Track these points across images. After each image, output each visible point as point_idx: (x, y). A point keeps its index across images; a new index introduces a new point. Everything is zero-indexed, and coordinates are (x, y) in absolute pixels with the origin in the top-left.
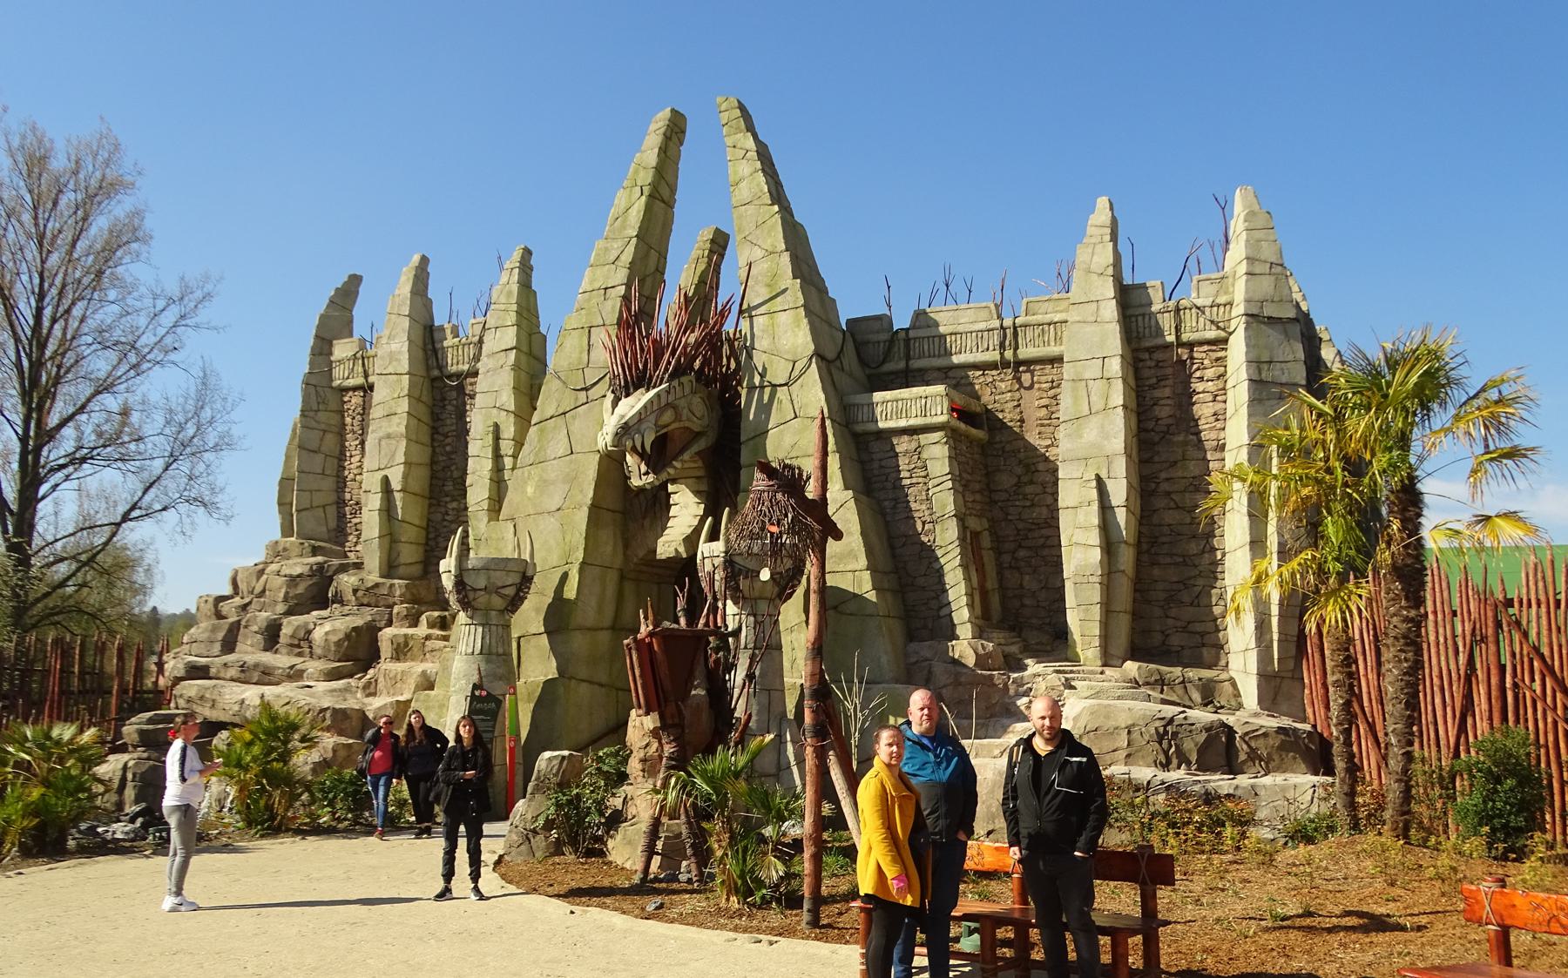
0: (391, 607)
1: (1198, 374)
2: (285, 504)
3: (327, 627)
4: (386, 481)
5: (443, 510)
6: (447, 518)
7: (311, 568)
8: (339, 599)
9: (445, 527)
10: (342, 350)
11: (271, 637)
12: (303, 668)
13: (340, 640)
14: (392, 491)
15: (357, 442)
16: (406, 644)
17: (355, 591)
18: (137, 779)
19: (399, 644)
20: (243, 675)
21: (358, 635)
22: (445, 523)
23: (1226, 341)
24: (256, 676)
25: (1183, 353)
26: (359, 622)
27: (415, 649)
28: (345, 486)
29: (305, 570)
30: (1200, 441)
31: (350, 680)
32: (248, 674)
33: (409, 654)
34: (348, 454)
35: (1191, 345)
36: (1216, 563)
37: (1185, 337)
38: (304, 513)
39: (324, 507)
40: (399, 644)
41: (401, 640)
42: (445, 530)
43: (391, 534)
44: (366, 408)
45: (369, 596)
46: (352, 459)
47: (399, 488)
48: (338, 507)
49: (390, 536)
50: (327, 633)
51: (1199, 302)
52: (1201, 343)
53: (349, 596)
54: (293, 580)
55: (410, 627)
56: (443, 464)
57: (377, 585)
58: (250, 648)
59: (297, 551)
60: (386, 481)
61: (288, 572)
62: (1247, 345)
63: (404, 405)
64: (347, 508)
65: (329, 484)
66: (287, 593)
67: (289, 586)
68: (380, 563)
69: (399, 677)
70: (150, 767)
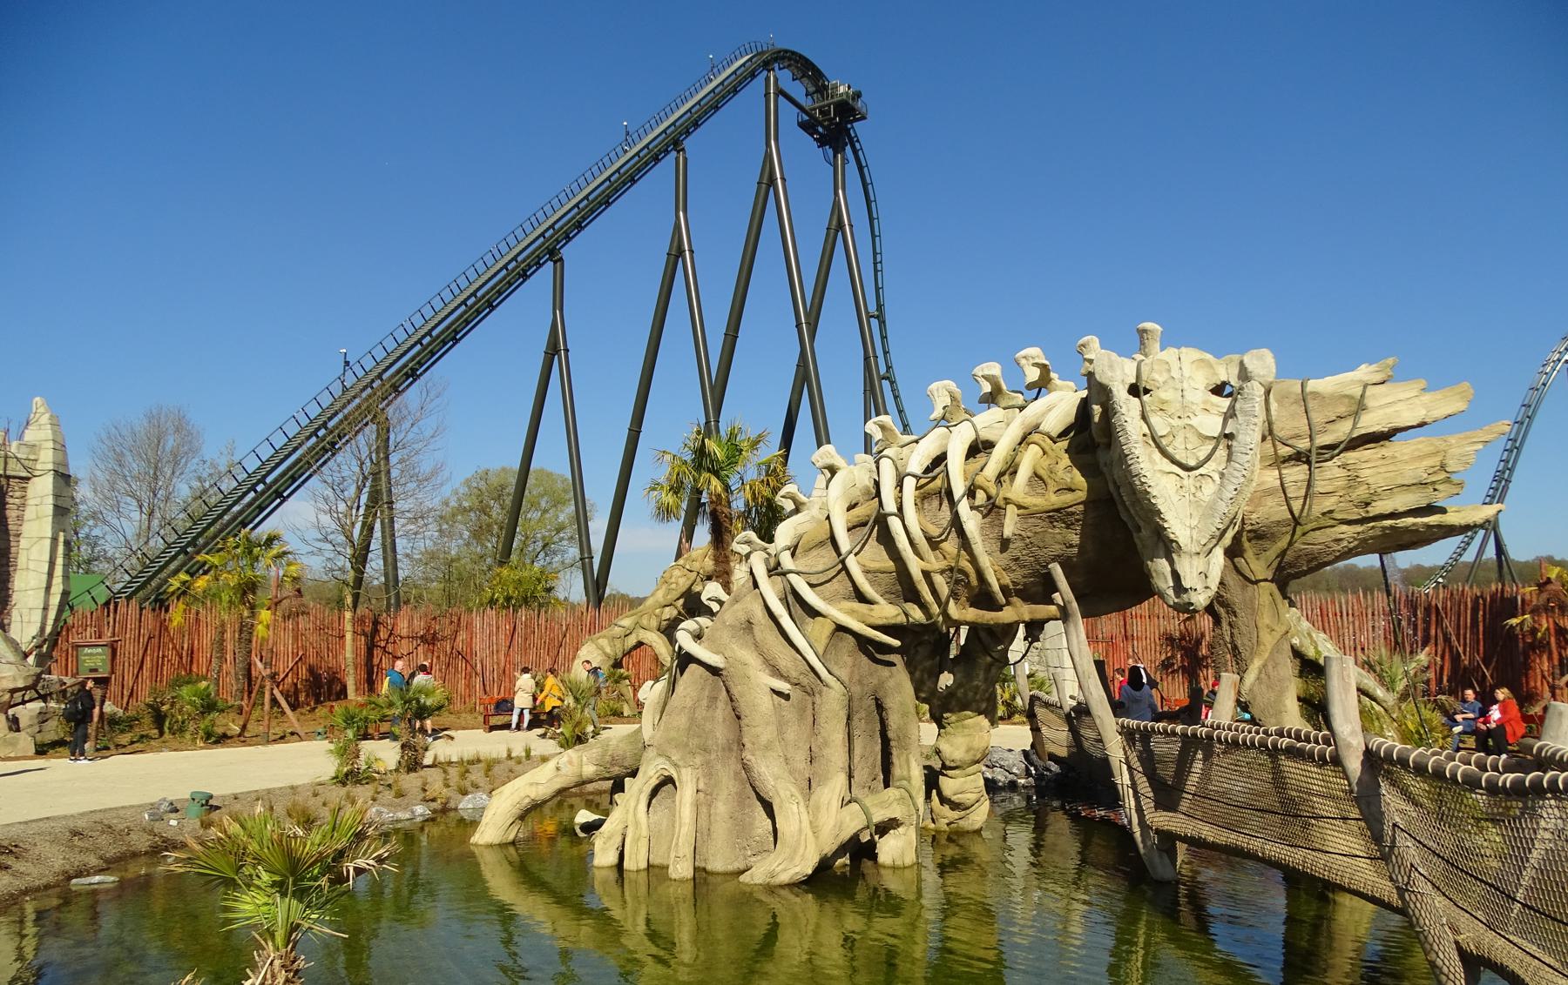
1: (11, 494)
23: (29, 479)
25: (4, 482)
30: (7, 529)
35: (8, 477)
36: (10, 596)
37: (8, 473)
51: (19, 456)
52: (15, 477)
62: (54, 487)
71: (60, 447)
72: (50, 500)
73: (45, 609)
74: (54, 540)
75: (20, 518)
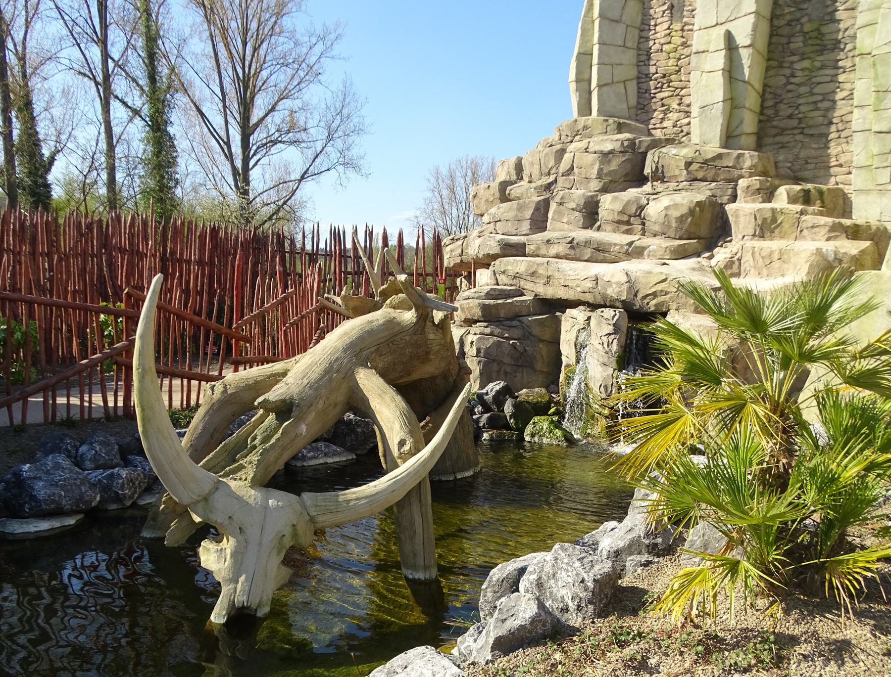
0: (735, 181)
2: (583, 80)
3: (665, 201)
4: (729, 37)
5: (787, 72)
6: (793, 80)
7: (622, 144)
8: (659, 176)
9: (789, 91)
12: (644, 245)
13: (682, 216)
14: (737, 48)
15: (665, 7)
16: (774, 220)
17: (688, 164)
18: (482, 355)
19: (765, 220)
20: (572, 252)
21: (702, 211)
22: (790, 87)
24: (588, 253)
26: (701, 197)
27: (786, 226)
28: (649, 59)
29: (617, 146)
31: (699, 259)
32: (577, 250)
33: (777, 231)
34: (652, 23)
38: (605, 89)
39: (624, 82)
40: (765, 220)
41: (768, 215)
42: (790, 95)
43: (731, 99)
46: (658, 28)
47: (748, 42)
48: (638, 83)
49: (732, 103)
50: (667, 208)
53: (676, 169)
54: (606, 156)
55: (763, 202)
56: (788, 17)
57: (719, 156)
58: (566, 226)
59: (601, 128)
60: (729, 37)
61: (597, 148)
64: (651, 83)
65: (629, 57)
66: (600, 170)
67: (601, 163)
68: (721, 131)
69: (776, 256)
70: (494, 343)
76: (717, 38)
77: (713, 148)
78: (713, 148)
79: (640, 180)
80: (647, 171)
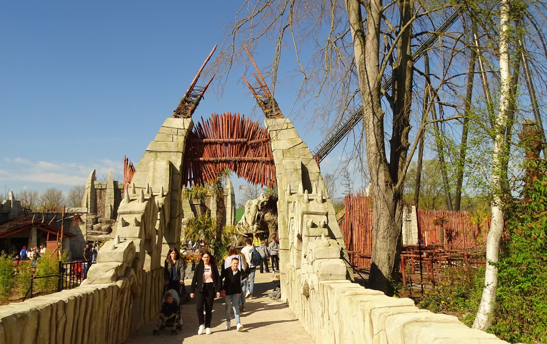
10: (95, 183)
11: (92, 228)
44: (101, 193)
45: (108, 222)
54: (93, 219)
63: (113, 193)
65: (94, 204)
71: (232, 188)
72: (230, 200)
73: (231, 222)
74: (232, 208)
75: (226, 204)
76: (109, 205)
77: (109, 219)
78: (109, 219)
79: (97, 223)
80: (99, 221)
